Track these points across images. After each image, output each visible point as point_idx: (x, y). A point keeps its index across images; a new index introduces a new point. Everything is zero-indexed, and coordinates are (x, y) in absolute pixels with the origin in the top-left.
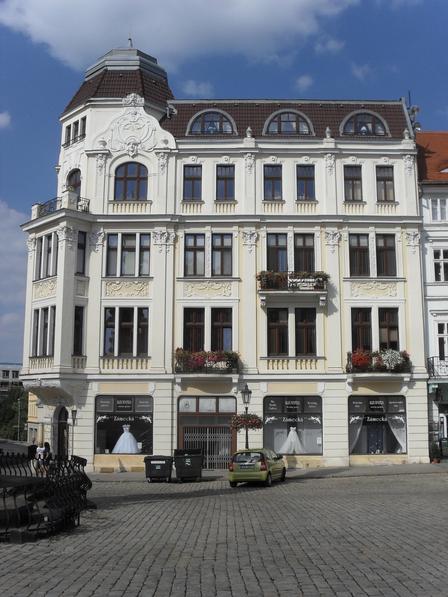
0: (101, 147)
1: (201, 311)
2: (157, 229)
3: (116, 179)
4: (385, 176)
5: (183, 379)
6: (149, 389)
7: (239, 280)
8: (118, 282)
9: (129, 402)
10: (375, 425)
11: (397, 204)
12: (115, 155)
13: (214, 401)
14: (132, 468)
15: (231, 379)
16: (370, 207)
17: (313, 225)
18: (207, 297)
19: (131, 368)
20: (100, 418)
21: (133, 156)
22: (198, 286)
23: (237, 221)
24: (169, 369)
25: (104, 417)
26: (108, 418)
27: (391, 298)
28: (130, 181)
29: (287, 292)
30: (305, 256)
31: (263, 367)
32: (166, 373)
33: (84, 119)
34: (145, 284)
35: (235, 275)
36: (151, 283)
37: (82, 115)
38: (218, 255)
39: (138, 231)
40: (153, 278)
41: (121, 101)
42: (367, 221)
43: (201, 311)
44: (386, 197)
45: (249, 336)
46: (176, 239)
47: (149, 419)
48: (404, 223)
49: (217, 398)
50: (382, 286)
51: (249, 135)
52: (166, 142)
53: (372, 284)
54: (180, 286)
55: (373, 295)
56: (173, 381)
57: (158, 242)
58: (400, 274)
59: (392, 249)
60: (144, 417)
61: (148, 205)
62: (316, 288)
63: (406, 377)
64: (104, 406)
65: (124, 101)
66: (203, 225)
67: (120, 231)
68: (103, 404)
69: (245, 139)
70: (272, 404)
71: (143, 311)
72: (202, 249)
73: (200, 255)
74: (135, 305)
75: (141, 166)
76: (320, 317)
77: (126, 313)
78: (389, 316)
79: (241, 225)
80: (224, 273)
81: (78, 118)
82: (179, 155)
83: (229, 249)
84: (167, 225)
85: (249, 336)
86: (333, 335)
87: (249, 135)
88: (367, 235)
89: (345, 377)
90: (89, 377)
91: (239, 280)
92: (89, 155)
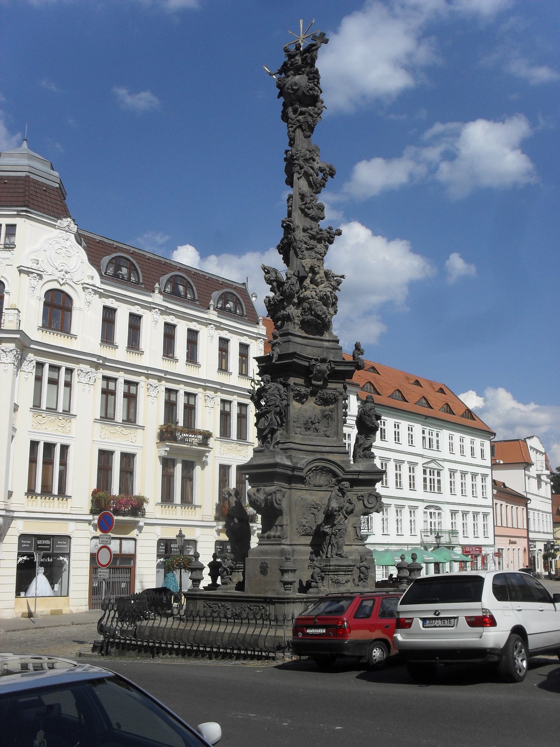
0: (35, 266)
1: (110, 453)
2: (82, 366)
3: (46, 304)
7: (143, 428)
8: (44, 415)
9: (47, 542)
11: (199, 366)
12: (46, 278)
13: (118, 542)
17: (139, 374)
18: (118, 441)
19: (52, 506)
20: (21, 559)
23: (146, 372)
25: (25, 558)
26: (28, 559)
28: (57, 309)
29: (186, 446)
34: (68, 421)
35: (140, 422)
36: (73, 420)
37: (11, 221)
39: (64, 365)
40: (76, 416)
41: (56, 222)
43: (110, 453)
45: (147, 481)
47: (65, 559)
49: (121, 539)
51: (157, 291)
52: (92, 278)
53: (233, 445)
57: (82, 380)
60: (61, 558)
62: (200, 445)
64: (25, 545)
65: (59, 223)
66: (118, 370)
67: (48, 361)
68: (24, 543)
69: (154, 294)
70: (162, 546)
71: (65, 448)
72: (113, 393)
73: (111, 398)
74: (59, 441)
76: (198, 468)
77: (49, 447)
79: (148, 376)
80: (130, 419)
87: (157, 291)
88: (230, 402)
89: (214, 524)
90: (16, 514)
91: (143, 428)
92: (21, 271)
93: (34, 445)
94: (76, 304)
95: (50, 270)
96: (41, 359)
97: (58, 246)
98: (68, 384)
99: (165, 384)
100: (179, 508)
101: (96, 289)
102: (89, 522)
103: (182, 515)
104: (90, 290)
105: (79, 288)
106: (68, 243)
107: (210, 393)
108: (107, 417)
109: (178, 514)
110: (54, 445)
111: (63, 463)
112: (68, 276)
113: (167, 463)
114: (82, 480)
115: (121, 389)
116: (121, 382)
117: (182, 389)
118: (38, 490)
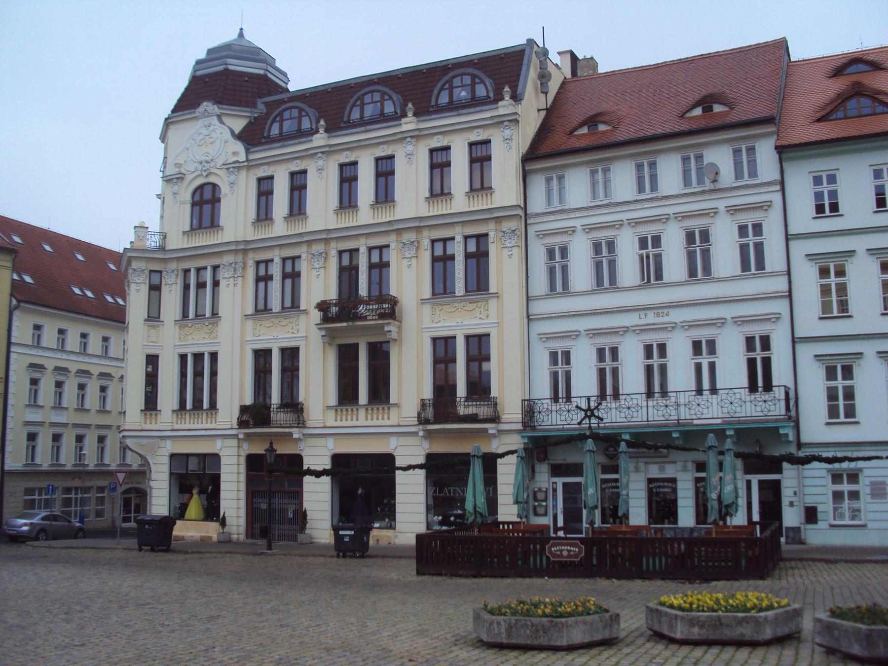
2: (228, 259)
3: (194, 204)
5: (245, 434)
6: (216, 447)
14: (201, 537)
15: (291, 434)
16: (460, 200)
18: (275, 336)
21: (207, 176)
22: (266, 323)
24: (235, 422)
27: (482, 321)
32: (232, 429)
38: (288, 282)
39: (209, 263)
44: (480, 185)
45: (318, 381)
46: (244, 268)
48: (498, 217)
50: (471, 306)
54: (249, 324)
55: (460, 321)
56: (235, 436)
61: (220, 232)
63: (491, 428)
67: (192, 265)
71: (214, 356)
74: (206, 350)
75: (214, 186)
78: (479, 346)
82: (249, 166)
84: (236, 251)
85: (318, 381)
93: (183, 358)
94: (225, 189)
96: (186, 265)
97: (202, 137)
98: (216, 284)
100: (362, 412)
101: (237, 165)
102: (235, 436)
103: (367, 420)
104: (231, 170)
105: (222, 173)
106: (212, 128)
107: (318, 248)
108: (262, 310)
109: (362, 419)
110: (202, 354)
111: (214, 374)
112: (212, 164)
114: (235, 388)
115: (276, 270)
118: (189, 405)
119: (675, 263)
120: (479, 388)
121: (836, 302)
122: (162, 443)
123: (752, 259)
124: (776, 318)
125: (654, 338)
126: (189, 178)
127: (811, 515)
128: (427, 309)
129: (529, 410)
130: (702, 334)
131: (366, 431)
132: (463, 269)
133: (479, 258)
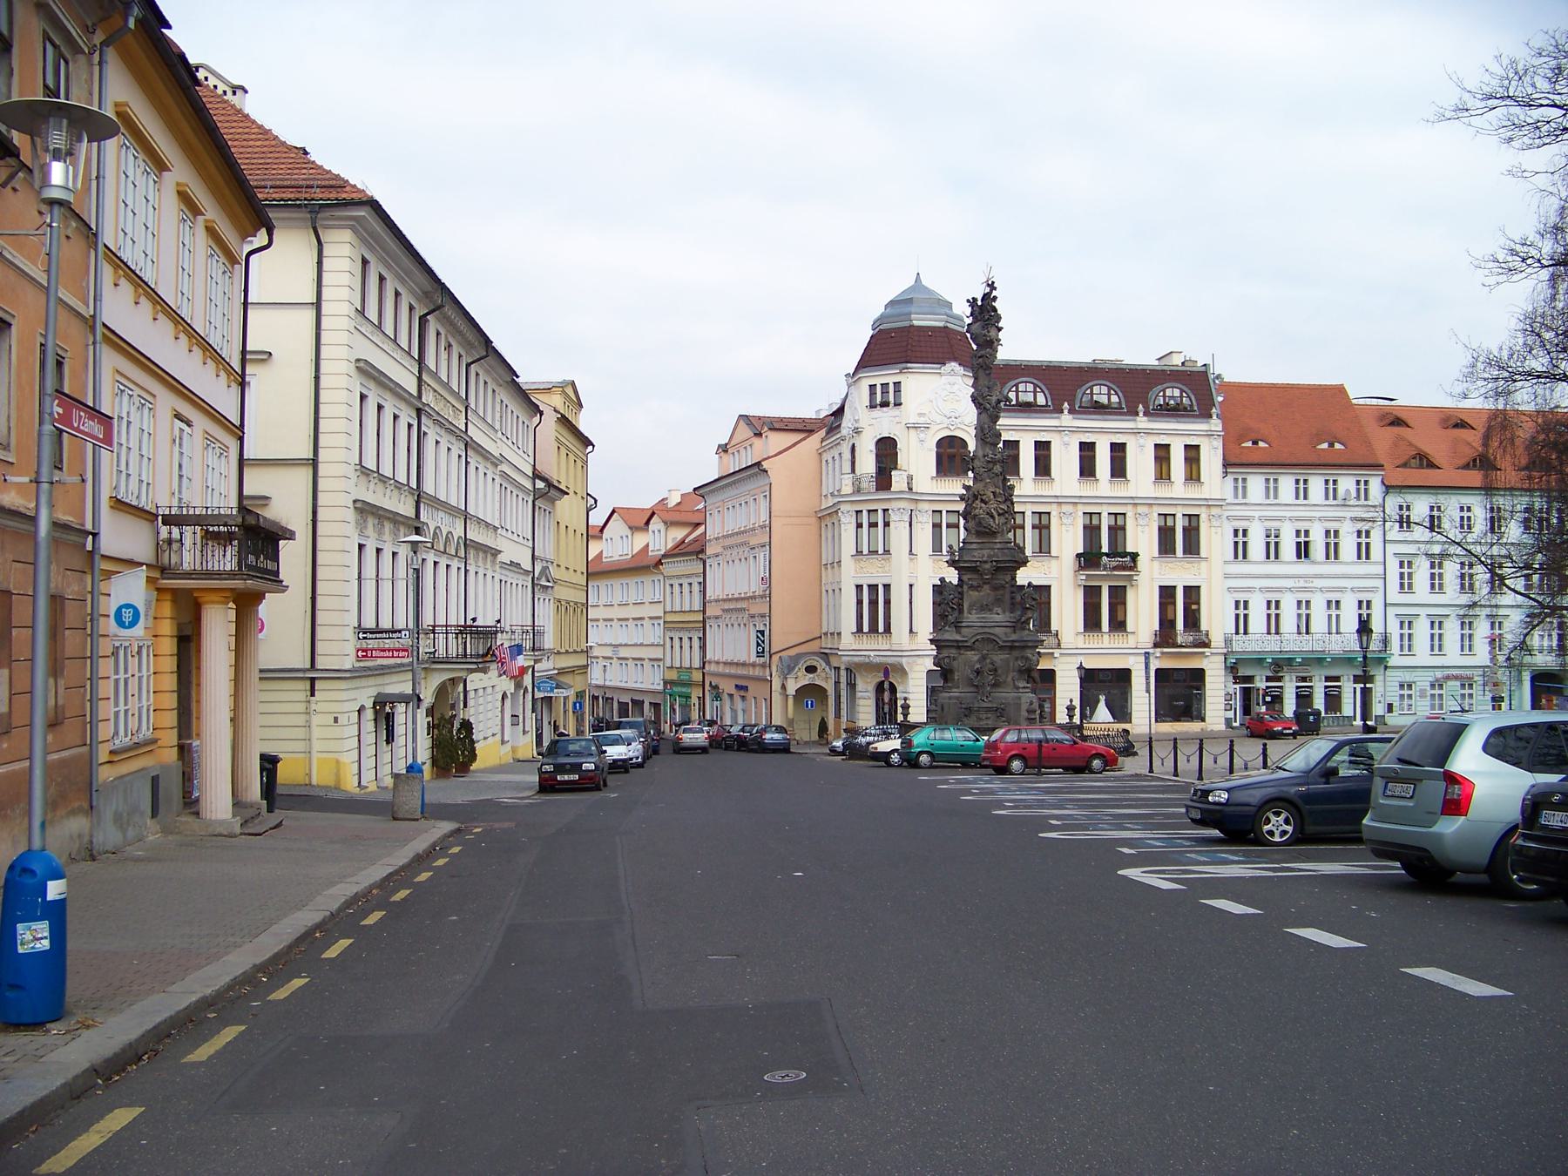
0: (922, 420)
4: (1192, 453)
10: (1180, 694)
30: (1117, 531)
31: (1080, 642)
33: (897, 384)
42: (1173, 501)
44: (1193, 475)
55: (1179, 574)
58: (1203, 554)
59: (1197, 529)
72: (1023, 527)
78: (1192, 593)
81: (891, 380)
83: (1048, 527)
86: (1143, 613)
95: (938, 419)
99: (1081, 509)
100: (1106, 637)
113: (1091, 594)
116: (1028, 514)
117: (1105, 511)
119: (1318, 550)
120: (1192, 620)
121: (1406, 584)
122: (920, 660)
123: (1364, 552)
124: (1372, 590)
125: (1304, 597)
126: (934, 428)
127: (1390, 708)
128: (1156, 564)
129: (1228, 641)
130: (1334, 597)
131: (1106, 652)
132: (1181, 537)
133: (1192, 533)
